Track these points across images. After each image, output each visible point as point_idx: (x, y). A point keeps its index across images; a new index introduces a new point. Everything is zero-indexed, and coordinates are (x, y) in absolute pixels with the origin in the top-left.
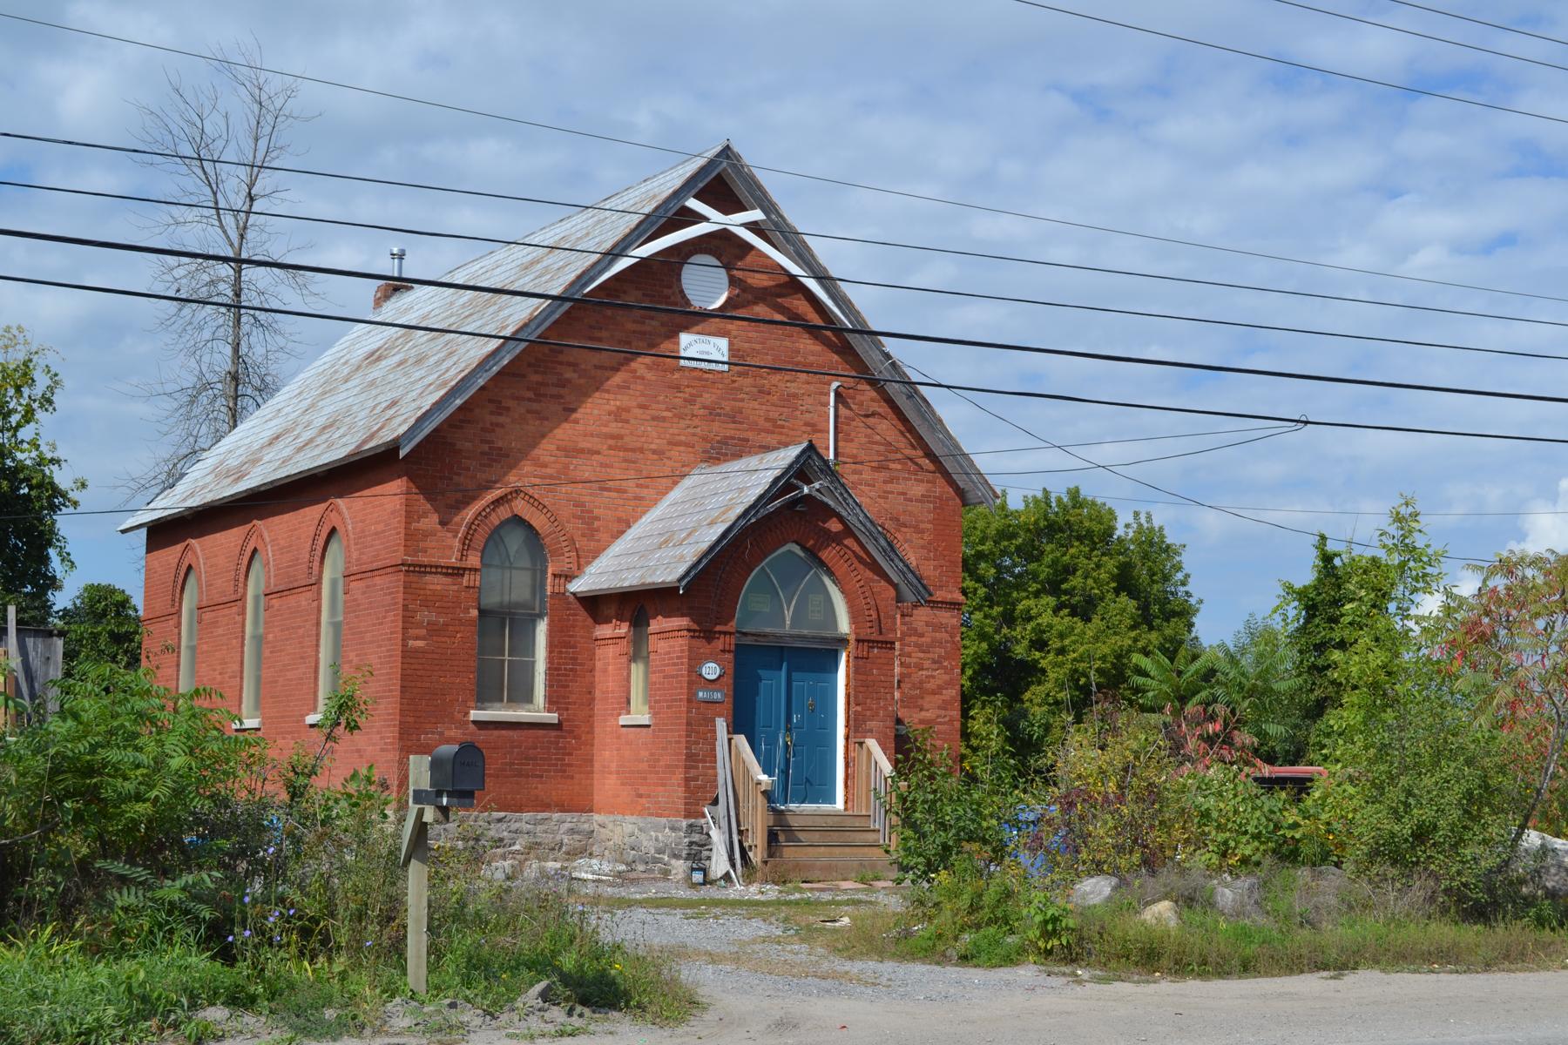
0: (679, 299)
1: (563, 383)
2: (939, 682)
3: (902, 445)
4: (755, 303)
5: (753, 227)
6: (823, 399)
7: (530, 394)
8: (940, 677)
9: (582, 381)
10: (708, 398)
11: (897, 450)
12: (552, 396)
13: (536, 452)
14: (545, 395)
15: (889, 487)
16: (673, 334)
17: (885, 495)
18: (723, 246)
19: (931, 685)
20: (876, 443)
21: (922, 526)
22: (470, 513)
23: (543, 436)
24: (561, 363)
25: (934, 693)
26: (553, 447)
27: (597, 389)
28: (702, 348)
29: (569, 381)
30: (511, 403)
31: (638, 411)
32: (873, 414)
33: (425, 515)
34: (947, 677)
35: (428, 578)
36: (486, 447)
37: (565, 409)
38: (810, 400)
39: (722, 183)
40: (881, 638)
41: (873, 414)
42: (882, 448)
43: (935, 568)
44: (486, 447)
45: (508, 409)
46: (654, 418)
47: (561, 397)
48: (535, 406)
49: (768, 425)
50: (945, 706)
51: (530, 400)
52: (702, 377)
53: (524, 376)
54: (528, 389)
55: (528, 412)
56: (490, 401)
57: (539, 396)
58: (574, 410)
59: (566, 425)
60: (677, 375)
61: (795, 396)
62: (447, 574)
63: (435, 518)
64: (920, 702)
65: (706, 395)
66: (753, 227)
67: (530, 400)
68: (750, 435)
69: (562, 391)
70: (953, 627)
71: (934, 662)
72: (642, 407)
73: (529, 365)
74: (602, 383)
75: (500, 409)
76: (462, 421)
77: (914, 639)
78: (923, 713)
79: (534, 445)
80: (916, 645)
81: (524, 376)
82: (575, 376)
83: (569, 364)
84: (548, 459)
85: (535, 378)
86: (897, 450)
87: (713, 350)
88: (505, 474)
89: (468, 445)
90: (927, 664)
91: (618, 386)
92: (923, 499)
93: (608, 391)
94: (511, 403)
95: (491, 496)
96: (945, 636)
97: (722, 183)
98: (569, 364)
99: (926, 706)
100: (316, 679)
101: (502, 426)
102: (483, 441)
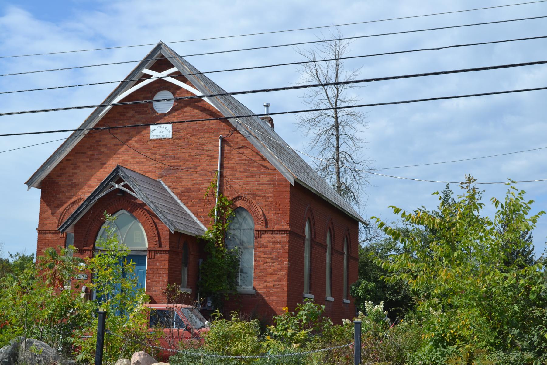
0: (151, 111)
1: (100, 153)
2: (275, 269)
3: (257, 159)
4: (186, 107)
5: (172, 75)
6: (216, 143)
7: (88, 160)
8: (276, 266)
9: (108, 152)
10: (162, 151)
11: (255, 162)
12: (96, 159)
13: (90, 182)
14: (93, 159)
15: (251, 179)
16: (147, 126)
17: (248, 183)
18: (161, 85)
19: (271, 271)
20: (242, 160)
21: (267, 195)
22: (61, 209)
23: (92, 175)
24: (100, 146)
25: (272, 274)
26: (96, 179)
27: (115, 154)
28: (160, 131)
29: (103, 152)
30: (80, 164)
31: (131, 160)
32: (242, 147)
33: (47, 211)
34: (279, 266)
35: (47, 235)
36: (70, 183)
37: (101, 164)
38: (210, 145)
39: (160, 60)
40: (160, 249)
41: (242, 147)
42: (246, 162)
43: (274, 215)
44: (70, 183)
45: (79, 167)
46: (138, 163)
47: (100, 159)
48: (89, 164)
49: (190, 158)
50: (279, 280)
51: (88, 162)
52: (160, 142)
53: (85, 153)
54: (87, 158)
55: (87, 167)
56: (72, 164)
57: (91, 160)
58: (105, 164)
59: (102, 170)
60: (149, 143)
61: (204, 144)
62: (53, 233)
63: (50, 212)
64: (265, 278)
65: (161, 150)
66: (172, 75)
67: (88, 162)
68: (181, 164)
69: (100, 157)
70: (284, 242)
71: (272, 259)
72: (132, 158)
73: (88, 148)
74: (116, 151)
75: (76, 167)
76: (61, 174)
77: (262, 249)
78: (266, 284)
79: (89, 180)
80: (263, 252)
81: (85, 153)
82: (106, 150)
83: (103, 145)
84: (93, 184)
85: (90, 153)
86: (255, 162)
87: (165, 130)
88: (77, 192)
89: (63, 182)
90: (269, 261)
91: (123, 151)
92: (269, 182)
93: (119, 154)
94: (80, 164)
95: (70, 202)
96: (279, 246)
97: (160, 60)
98: (103, 145)
99: (268, 280)
100: (348, 275)
101: (76, 173)
102: (69, 181)
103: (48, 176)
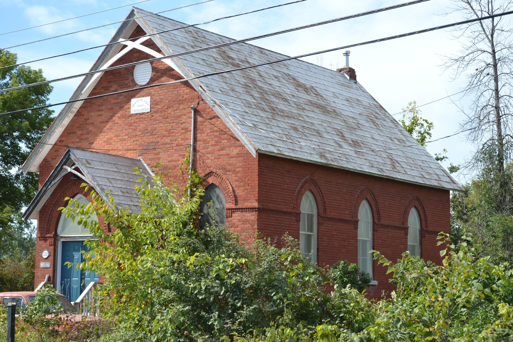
0: (131, 84)
4: (162, 77)
9: (95, 130)
10: (142, 126)
12: (85, 139)
14: (82, 139)
15: (222, 152)
17: (219, 157)
18: (135, 56)
20: (214, 131)
21: (237, 170)
24: (88, 124)
27: (101, 132)
28: (140, 105)
29: (91, 131)
31: (115, 138)
38: (184, 117)
42: (218, 133)
46: (121, 140)
47: (88, 138)
48: (79, 145)
51: (78, 142)
53: (75, 133)
54: (78, 138)
58: (92, 143)
60: (130, 118)
61: (179, 117)
65: (141, 125)
66: (143, 44)
68: (159, 139)
69: (88, 136)
70: (253, 221)
73: (78, 127)
74: (102, 129)
76: (56, 156)
81: (75, 133)
82: (93, 128)
85: (79, 132)
91: (108, 129)
93: (104, 132)
103: (45, 160)
